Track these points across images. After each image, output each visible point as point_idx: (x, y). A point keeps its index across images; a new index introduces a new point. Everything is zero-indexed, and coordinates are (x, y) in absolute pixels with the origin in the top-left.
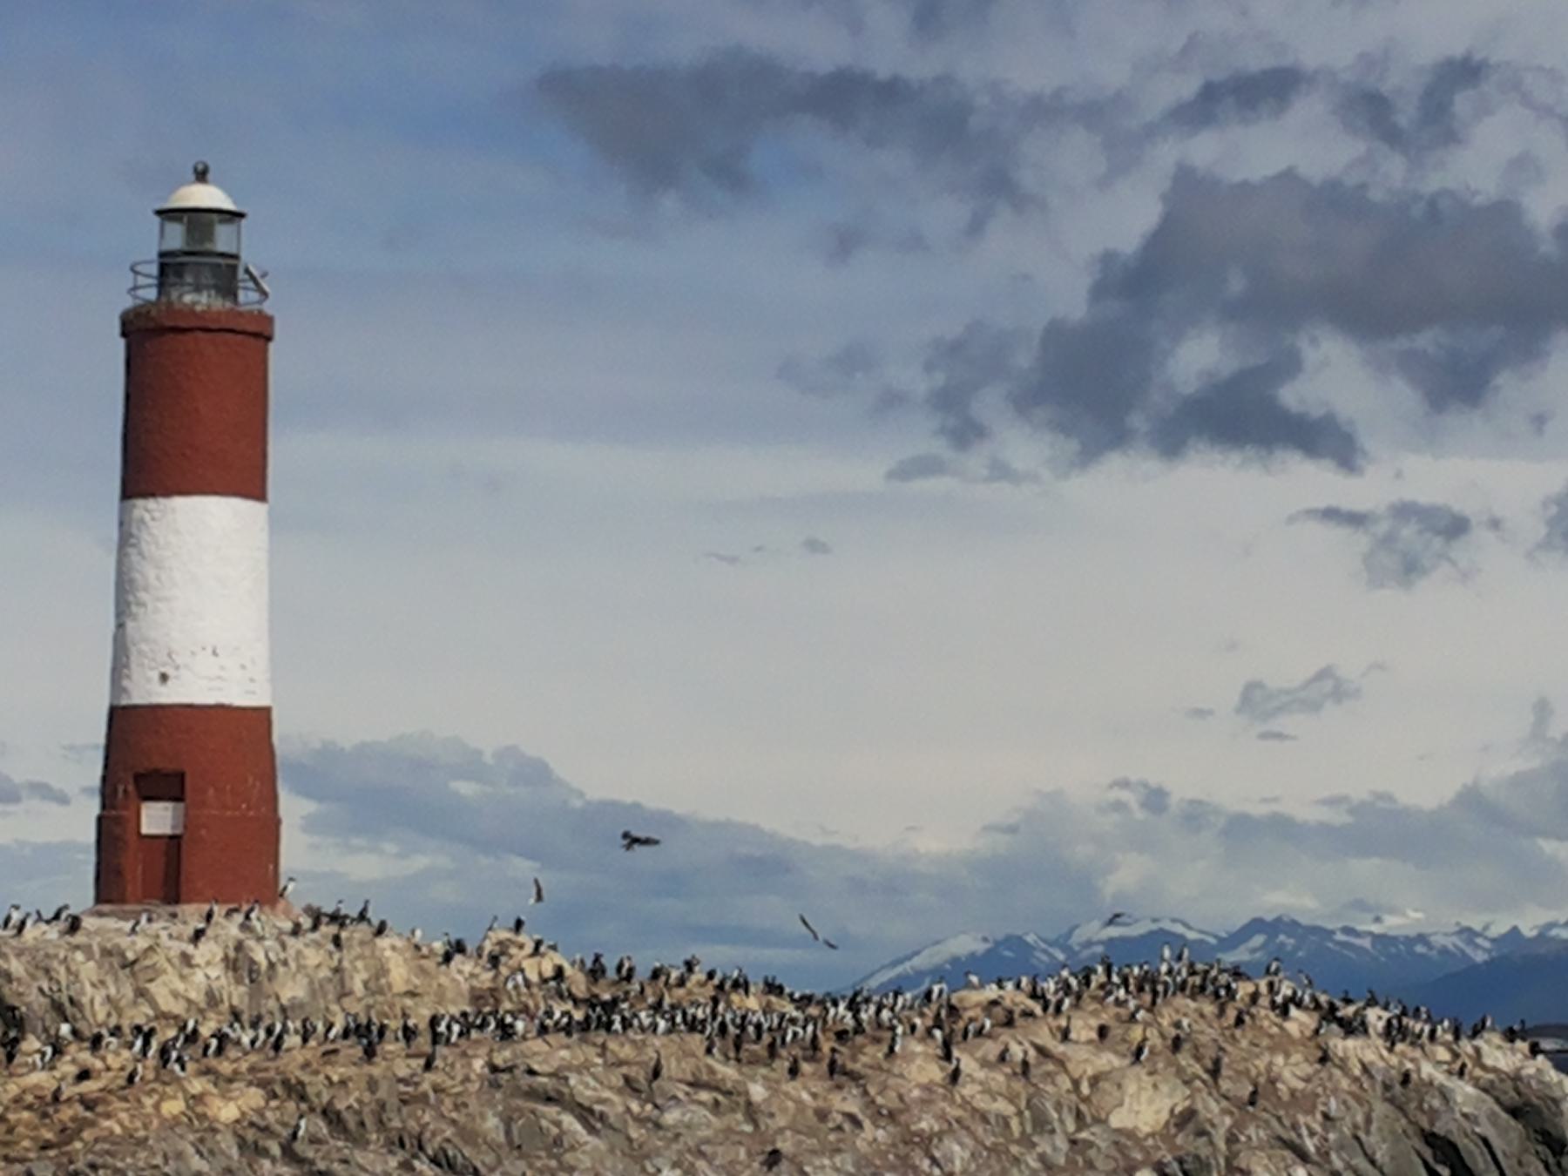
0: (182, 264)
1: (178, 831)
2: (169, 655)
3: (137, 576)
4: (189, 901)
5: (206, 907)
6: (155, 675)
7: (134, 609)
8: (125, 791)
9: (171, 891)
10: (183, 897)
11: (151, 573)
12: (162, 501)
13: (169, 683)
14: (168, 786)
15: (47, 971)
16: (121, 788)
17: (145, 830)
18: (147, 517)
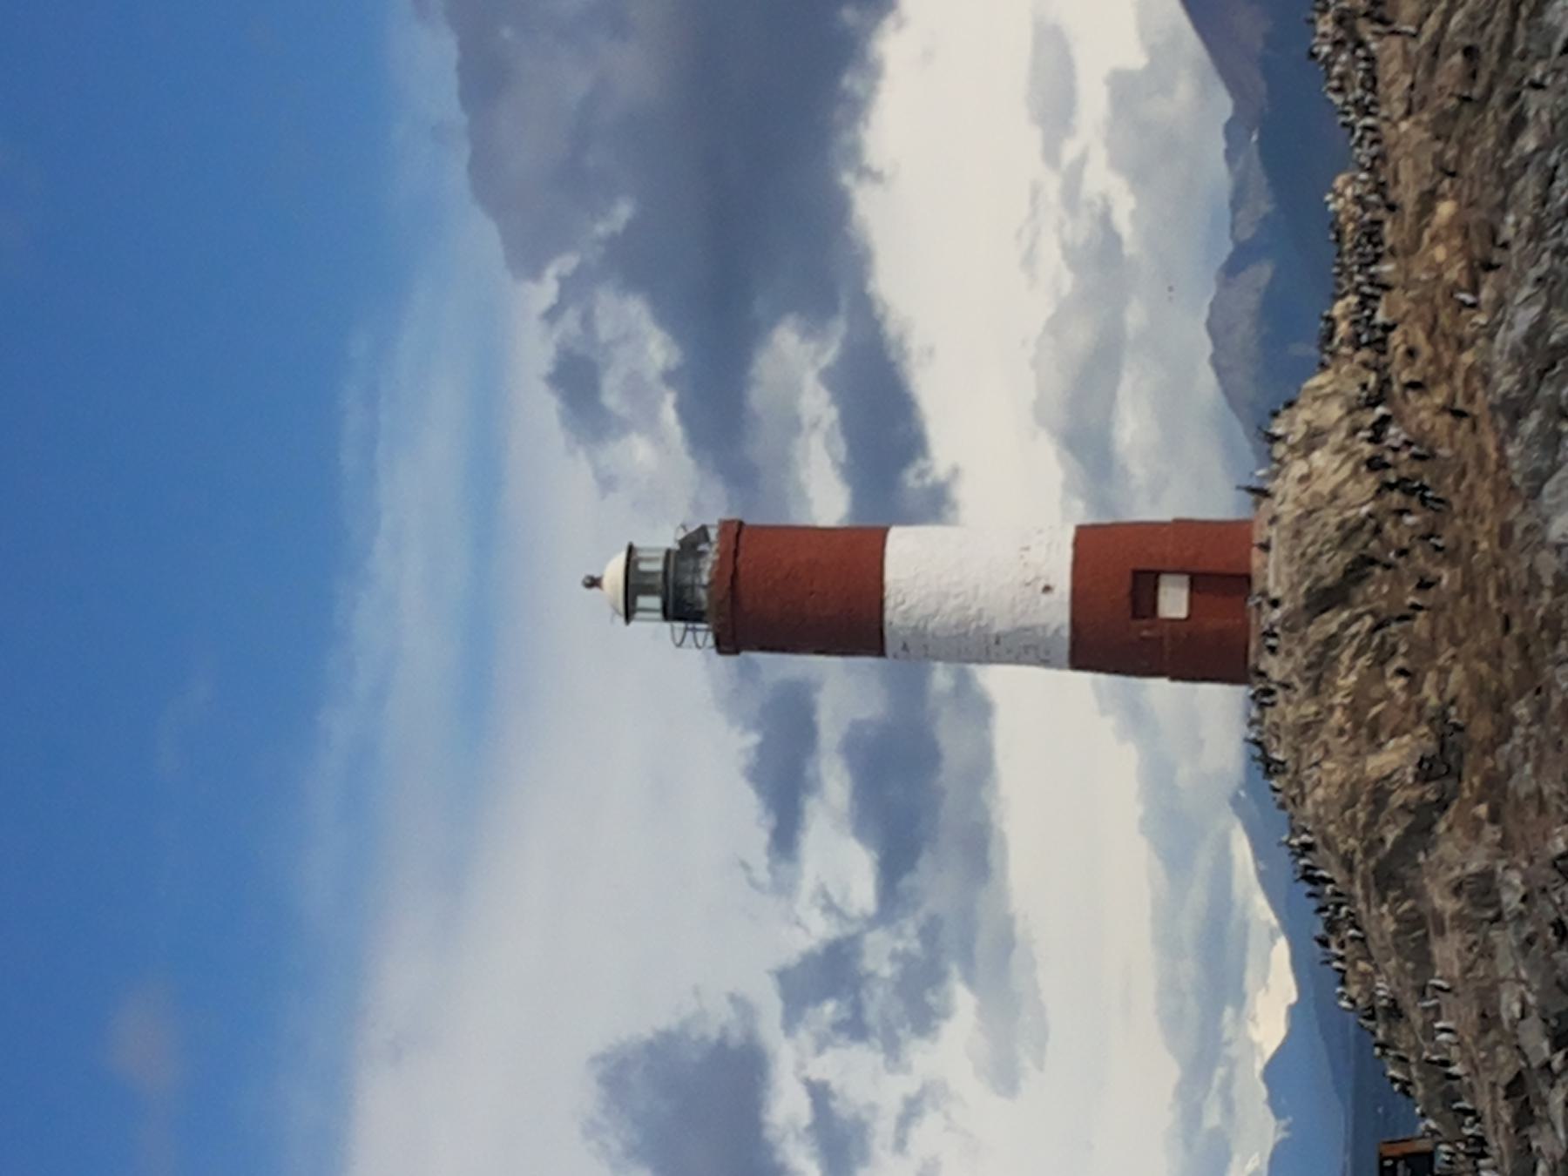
0: (675, 585)
1: (1185, 579)
2: (1028, 584)
3: (953, 621)
4: (1248, 565)
5: (1255, 551)
6: (1045, 598)
7: (983, 623)
8: (1148, 628)
9: (1241, 582)
10: (1244, 571)
11: (953, 603)
12: (886, 594)
13: (1051, 583)
14: (1144, 586)
15: (1313, 561)
16: (1145, 633)
17: (1181, 611)
18: (902, 608)
